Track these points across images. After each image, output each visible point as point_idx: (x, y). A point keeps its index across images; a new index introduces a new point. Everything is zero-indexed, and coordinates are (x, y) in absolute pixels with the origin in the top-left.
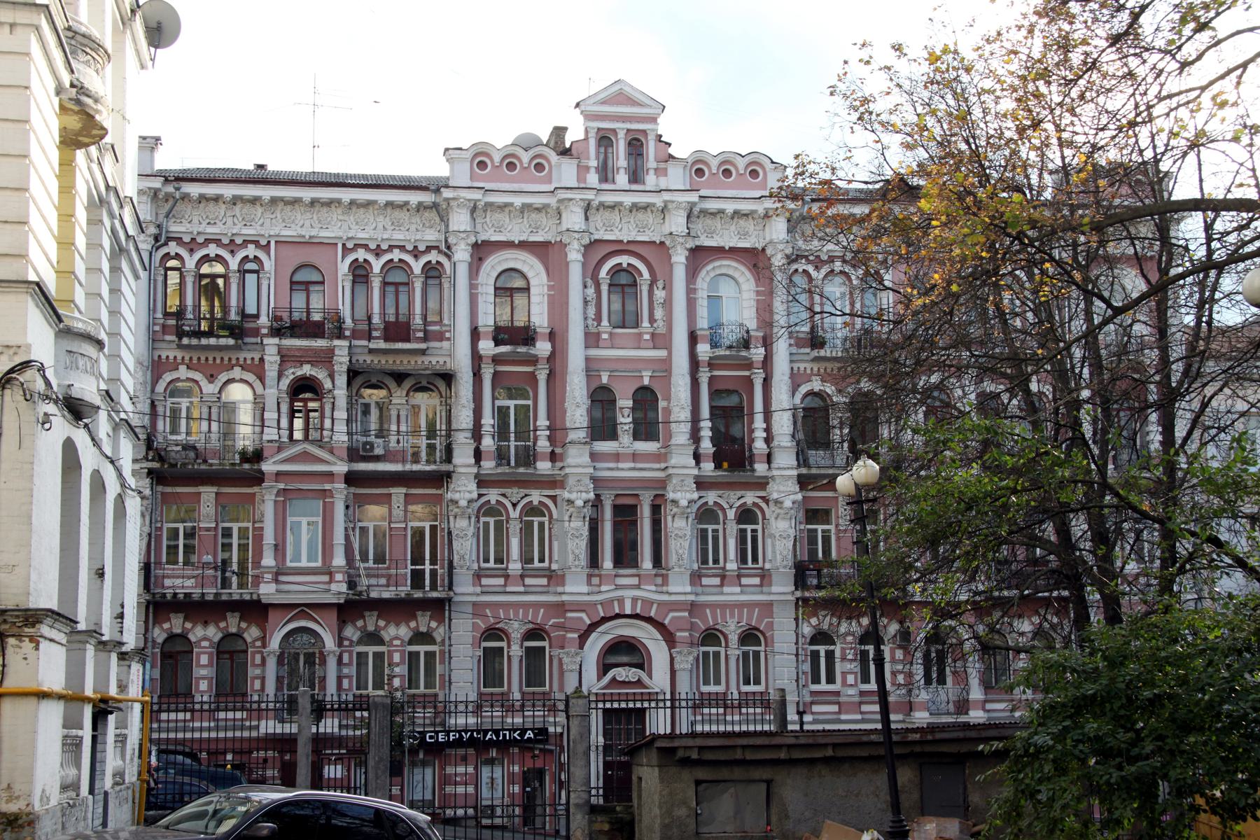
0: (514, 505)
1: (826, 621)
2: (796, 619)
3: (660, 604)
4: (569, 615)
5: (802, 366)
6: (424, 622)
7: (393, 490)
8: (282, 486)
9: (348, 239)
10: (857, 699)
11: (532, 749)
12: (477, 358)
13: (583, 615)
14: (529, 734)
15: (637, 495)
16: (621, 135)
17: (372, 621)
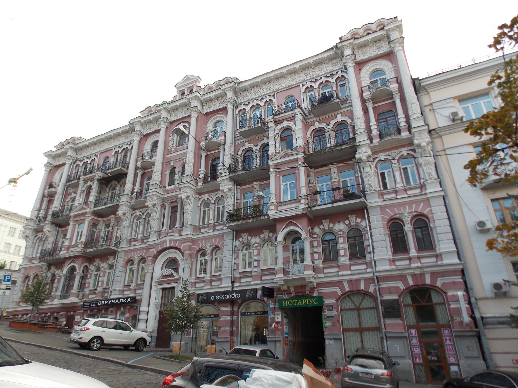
0: (143, 214)
1: (245, 238)
2: (233, 240)
3: (180, 240)
4: (150, 250)
5: (242, 141)
6: (111, 260)
7: (111, 216)
8: (75, 219)
9: (115, 146)
10: (261, 274)
11: (133, 306)
12: (137, 168)
13: (154, 250)
14: (129, 300)
15: (176, 201)
16: (186, 89)
17: (97, 262)
